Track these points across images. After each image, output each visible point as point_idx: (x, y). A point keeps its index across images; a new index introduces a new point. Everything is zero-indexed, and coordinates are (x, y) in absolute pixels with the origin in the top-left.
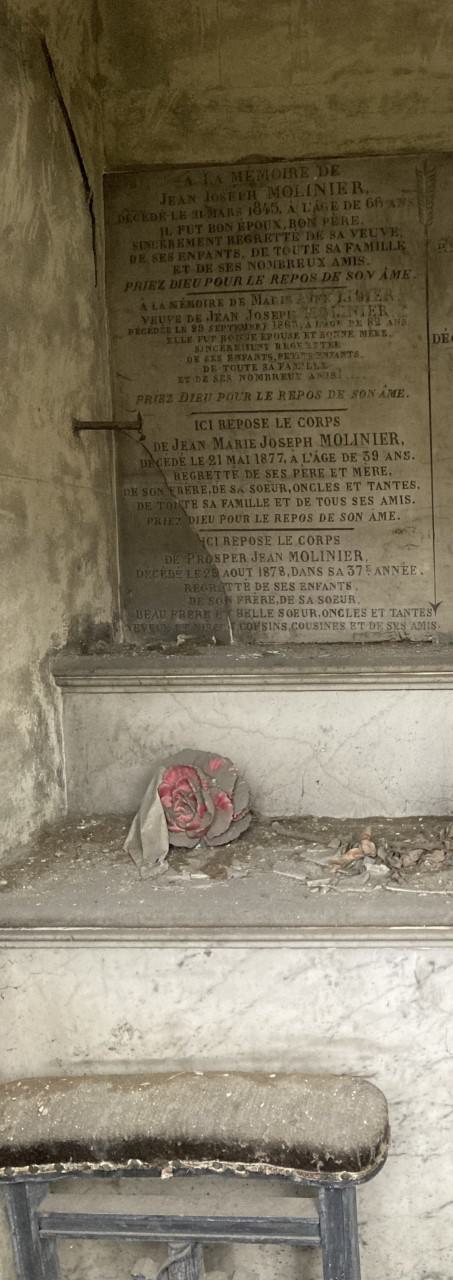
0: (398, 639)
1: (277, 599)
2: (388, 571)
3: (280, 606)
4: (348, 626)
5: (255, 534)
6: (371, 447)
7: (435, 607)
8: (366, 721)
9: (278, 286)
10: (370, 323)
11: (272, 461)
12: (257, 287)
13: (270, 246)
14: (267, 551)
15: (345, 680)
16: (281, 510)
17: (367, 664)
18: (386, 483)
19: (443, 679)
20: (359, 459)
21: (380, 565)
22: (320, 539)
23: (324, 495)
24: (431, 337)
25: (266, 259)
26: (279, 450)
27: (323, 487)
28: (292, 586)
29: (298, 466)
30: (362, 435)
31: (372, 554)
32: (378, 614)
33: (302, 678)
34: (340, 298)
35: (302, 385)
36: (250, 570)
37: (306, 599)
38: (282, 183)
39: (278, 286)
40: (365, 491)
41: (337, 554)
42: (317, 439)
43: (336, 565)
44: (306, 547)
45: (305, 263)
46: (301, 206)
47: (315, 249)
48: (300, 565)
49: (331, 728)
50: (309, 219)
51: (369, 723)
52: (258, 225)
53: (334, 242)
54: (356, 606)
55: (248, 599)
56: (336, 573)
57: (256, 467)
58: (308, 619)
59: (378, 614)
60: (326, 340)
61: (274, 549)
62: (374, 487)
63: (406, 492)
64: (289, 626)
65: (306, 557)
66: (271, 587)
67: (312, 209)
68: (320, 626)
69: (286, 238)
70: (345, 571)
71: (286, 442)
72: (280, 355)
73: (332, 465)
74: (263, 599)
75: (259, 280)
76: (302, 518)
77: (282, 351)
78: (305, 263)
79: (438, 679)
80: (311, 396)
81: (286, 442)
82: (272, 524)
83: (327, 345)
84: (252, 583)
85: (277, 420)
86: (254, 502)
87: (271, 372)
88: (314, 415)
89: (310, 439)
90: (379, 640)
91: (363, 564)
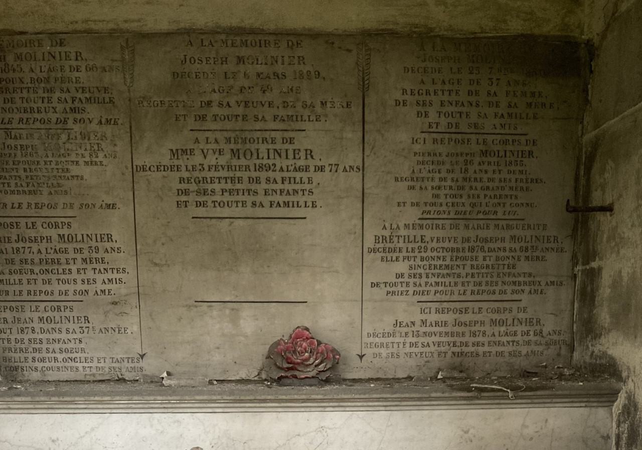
0: (117, 378)
1: (31, 350)
2: (108, 331)
3: (34, 355)
4: (81, 369)
5: (14, 304)
6: (93, 244)
7: (142, 356)
8: (82, 435)
9: (24, 126)
10: (91, 155)
11: (24, 253)
12: (8, 126)
13: (17, 96)
14: (23, 316)
15: (65, 406)
16: (32, 287)
17: (80, 395)
18: (105, 269)
19: (134, 406)
20: (86, 252)
21: (102, 327)
22: (59, 308)
23: (62, 277)
24: (135, 167)
25: (14, 106)
26: (28, 245)
27: (61, 271)
28: (41, 340)
29: (43, 256)
30: (88, 235)
31: (96, 320)
32: (102, 361)
33: (35, 404)
34: (69, 136)
35: (44, 199)
36: (11, 329)
37: (51, 350)
38: (24, 50)
39: (24, 126)
40: (90, 274)
41: (71, 319)
42: (55, 237)
43: (71, 326)
44: (50, 314)
45: (43, 110)
46: (38, 69)
47: (49, 100)
48: (46, 326)
49: (58, 439)
50: (45, 78)
51: (84, 436)
52: (8, 80)
53: (63, 96)
54: (86, 355)
55: (10, 349)
56: (71, 332)
57: (13, 256)
58: (53, 364)
59: (102, 361)
60: (60, 166)
61: (28, 314)
62: (97, 271)
63: (118, 276)
64: (39, 369)
65: (49, 320)
66: (26, 341)
67: (46, 70)
68: (61, 369)
69: (28, 91)
70: (78, 330)
71: (33, 239)
72: (27, 177)
73: (67, 256)
74: (21, 350)
75: (10, 122)
76: (47, 293)
77: (28, 174)
78: (43, 110)
79: (130, 406)
80: (51, 207)
81: (33, 239)
82: (25, 297)
83: (60, 171)
84: (13, 337)
85: (27, 223)
86: (12, 282)
87: (20, 189)
88: (53, 220)
89: (51, 237)
90: (104, 379)
91: (90, 325)
